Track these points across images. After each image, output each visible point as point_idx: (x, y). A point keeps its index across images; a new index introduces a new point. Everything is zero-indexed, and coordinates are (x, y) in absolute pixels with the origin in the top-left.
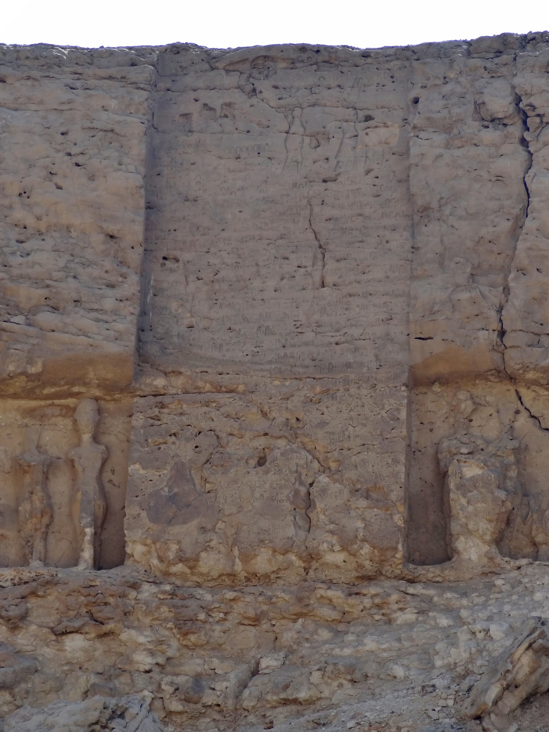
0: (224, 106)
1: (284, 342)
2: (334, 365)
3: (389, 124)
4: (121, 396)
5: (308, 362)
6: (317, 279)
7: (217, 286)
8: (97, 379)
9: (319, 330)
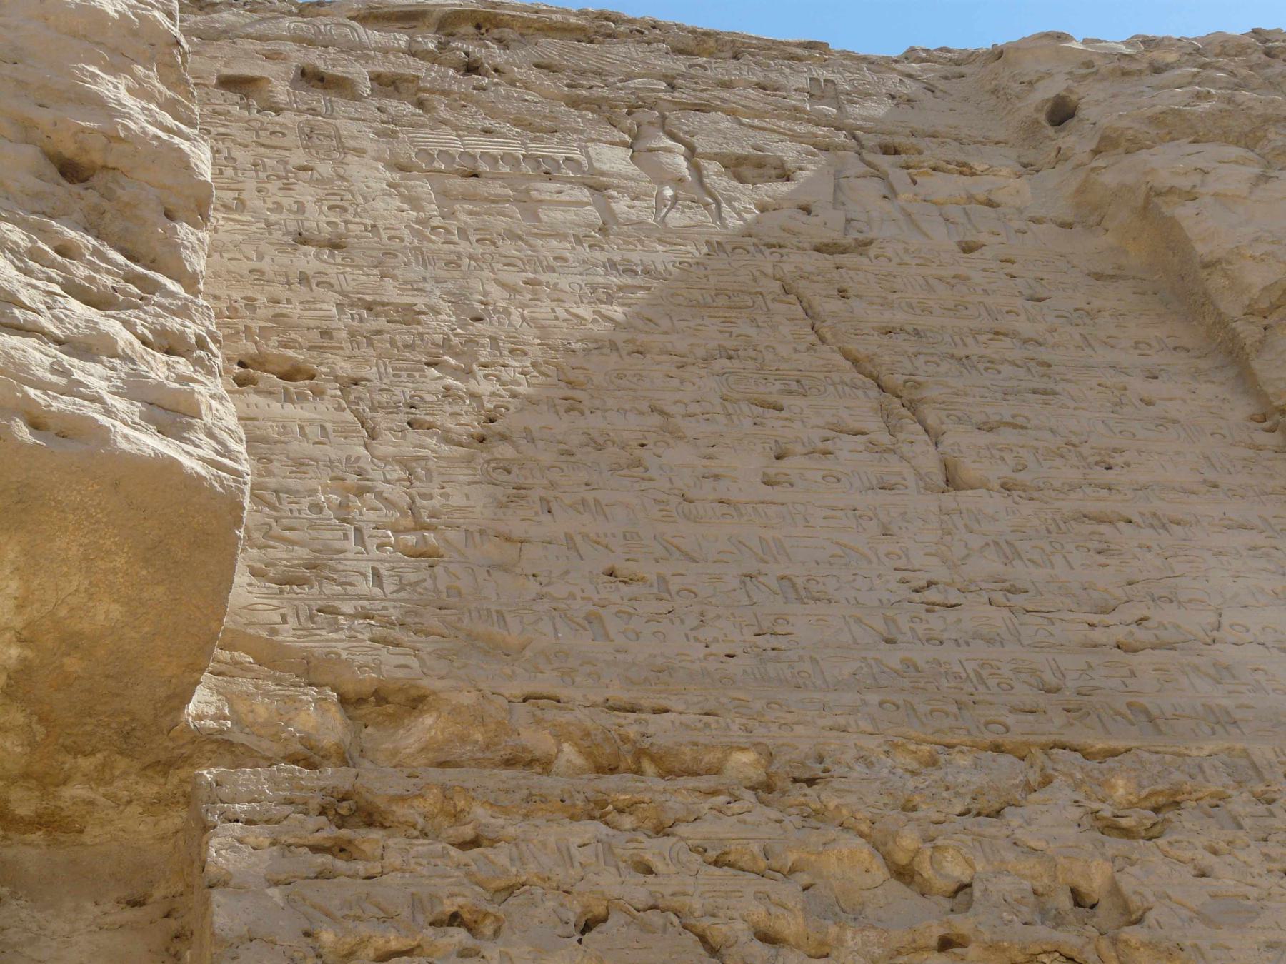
0: (375, 84)
1: (880, 625)
2: (1155, 712)
3: (979, 167)
4: (97, 795)
5: (1025, 694)
6: (929, 462)
7: (505, 451)
8: (21, 641)
9: (1017, 600)
